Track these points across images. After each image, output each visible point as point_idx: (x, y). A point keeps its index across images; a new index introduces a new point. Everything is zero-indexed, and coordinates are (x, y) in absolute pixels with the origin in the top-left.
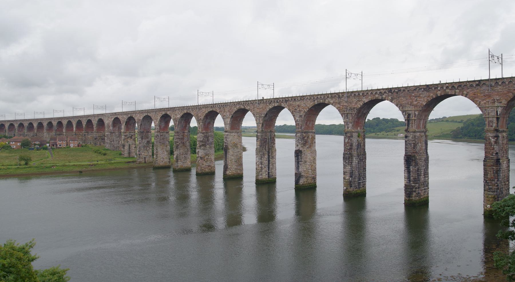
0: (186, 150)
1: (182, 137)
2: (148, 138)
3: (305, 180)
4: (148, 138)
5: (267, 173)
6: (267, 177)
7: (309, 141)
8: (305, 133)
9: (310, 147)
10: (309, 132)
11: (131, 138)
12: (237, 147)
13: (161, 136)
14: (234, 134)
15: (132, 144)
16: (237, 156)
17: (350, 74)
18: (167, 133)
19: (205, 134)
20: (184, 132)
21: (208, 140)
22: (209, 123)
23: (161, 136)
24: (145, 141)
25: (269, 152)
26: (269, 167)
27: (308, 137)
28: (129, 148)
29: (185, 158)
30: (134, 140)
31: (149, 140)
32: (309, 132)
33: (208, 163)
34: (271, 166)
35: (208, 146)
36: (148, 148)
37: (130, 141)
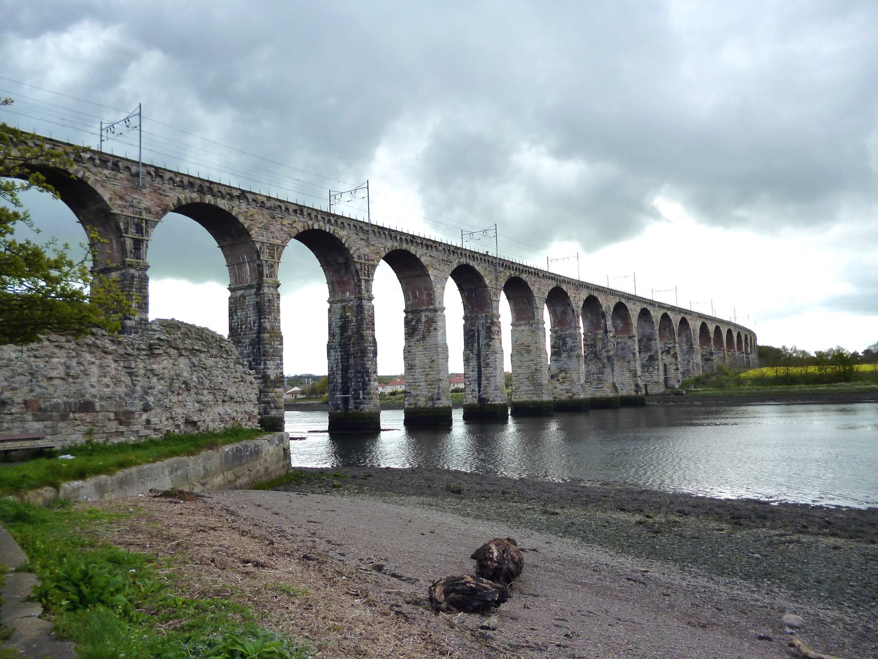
0: (601, 365)
1: (592, 342)
2: (650, 350)
3: (413, 401)
4: (650, 350)
5: (476, 394)
6: (476, 401)
7: (421, 327)
8: (413, 312)
9: (424, 338)
10: (422, 311)
11: (668, 352)
12: (529, 352)
13: (618, 343)
14: (523, 328)
15: (671, 364)
16: (529, 367)
17: (338, 197)
18: (630, 338)
19: (560, 333)
20: (596, 334)
21: (565, 344)
22: (564, 313)
23: (618, 343)
24: (646, 356)
25: (479, 356)
26: (479, 385)
27: (419, 321)
28: (665, 371)
29: (600, 380)
30: (675, 356)
31: (652, 353)
32: (422, 311)
33: (566, 386)
34: (484, 382)
35: (564, 355)
36: (651, 369)
37: (668, 359)
